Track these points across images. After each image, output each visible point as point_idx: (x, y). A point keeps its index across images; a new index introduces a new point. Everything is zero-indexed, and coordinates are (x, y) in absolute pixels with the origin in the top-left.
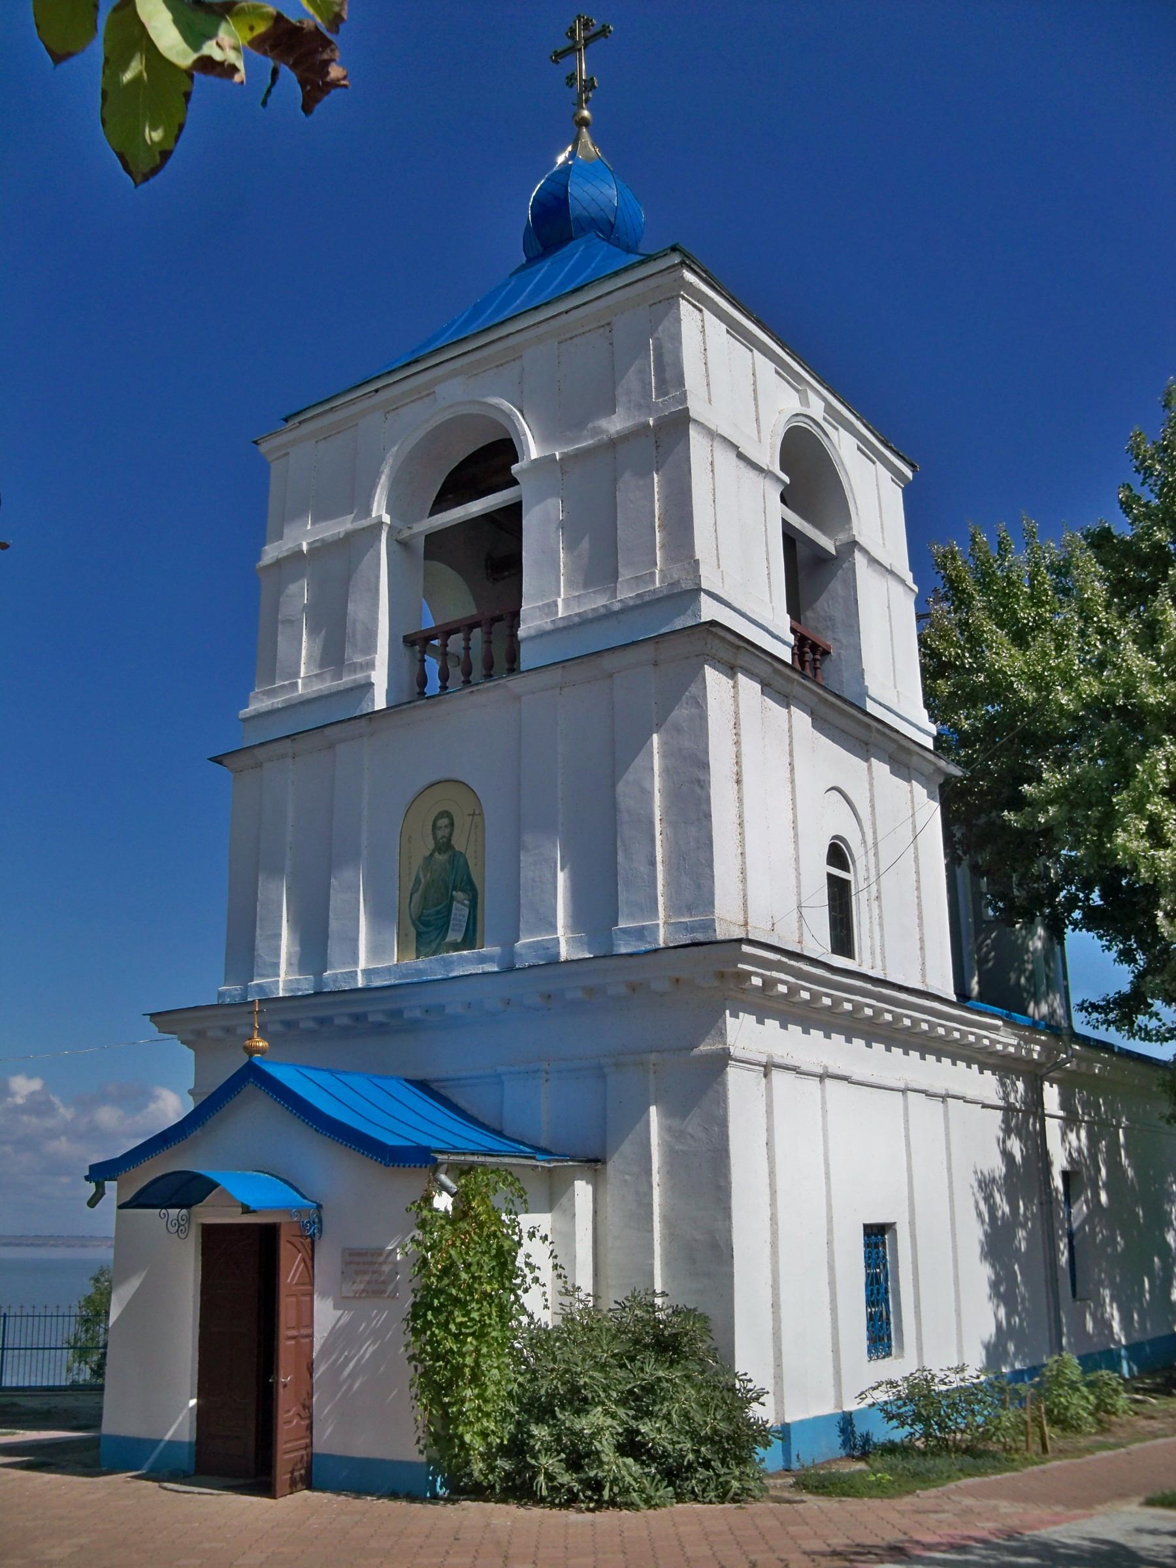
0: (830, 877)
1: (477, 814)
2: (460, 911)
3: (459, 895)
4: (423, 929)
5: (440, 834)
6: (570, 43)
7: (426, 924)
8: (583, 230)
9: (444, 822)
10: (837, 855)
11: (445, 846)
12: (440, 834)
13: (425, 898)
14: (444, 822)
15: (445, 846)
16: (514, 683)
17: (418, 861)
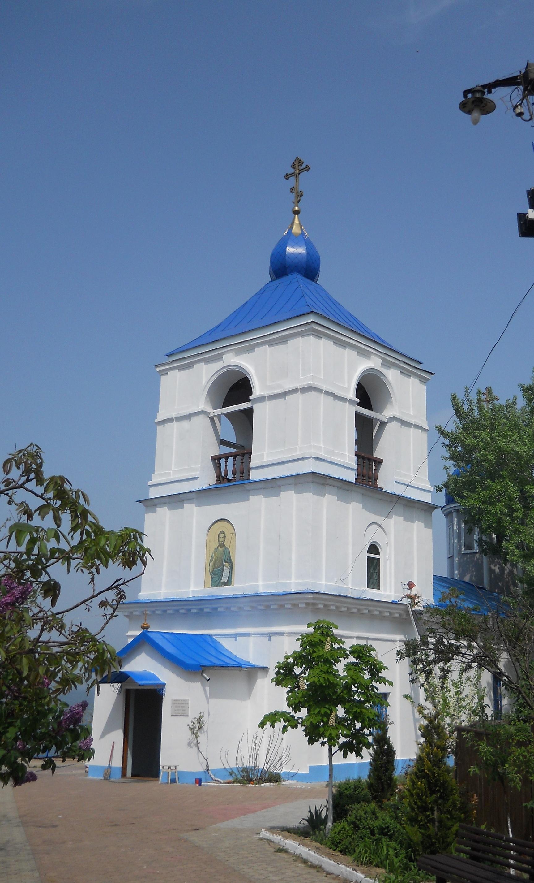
0: (369, 558)
1: (234, 533)
2: (226, 571)
3: (226, 564)
4: (213, 576)
5: (221, 540)
6: (292, 171)
7: (215, 574)
8: (292, 271)
9: (222, 535)
10: (373, 548)
11: (222, 545)
12: (221, 540)
13: (214, 564)
14: (222, 535)
15: (222, 545)
16: (248, 487)
17: (213, 550)
